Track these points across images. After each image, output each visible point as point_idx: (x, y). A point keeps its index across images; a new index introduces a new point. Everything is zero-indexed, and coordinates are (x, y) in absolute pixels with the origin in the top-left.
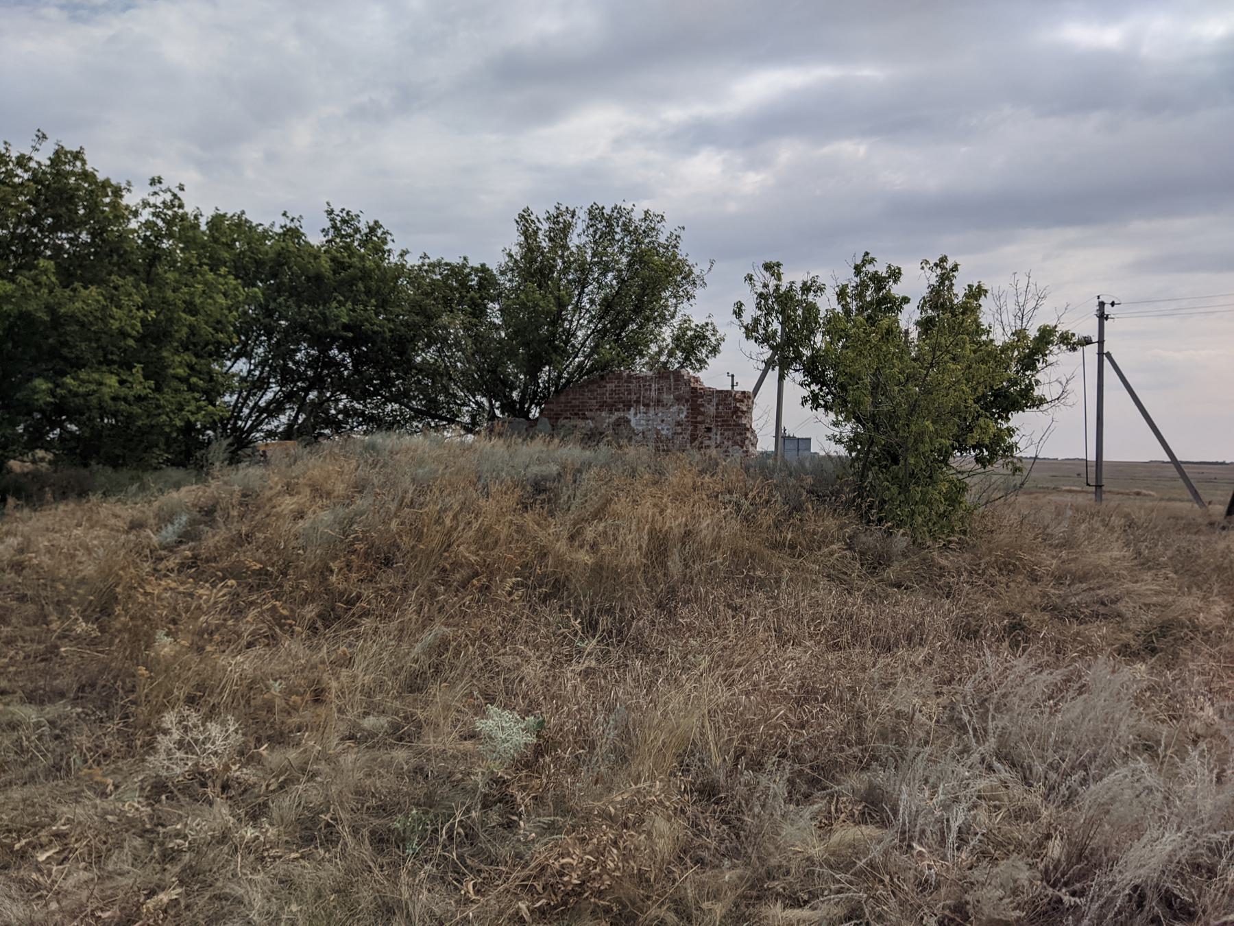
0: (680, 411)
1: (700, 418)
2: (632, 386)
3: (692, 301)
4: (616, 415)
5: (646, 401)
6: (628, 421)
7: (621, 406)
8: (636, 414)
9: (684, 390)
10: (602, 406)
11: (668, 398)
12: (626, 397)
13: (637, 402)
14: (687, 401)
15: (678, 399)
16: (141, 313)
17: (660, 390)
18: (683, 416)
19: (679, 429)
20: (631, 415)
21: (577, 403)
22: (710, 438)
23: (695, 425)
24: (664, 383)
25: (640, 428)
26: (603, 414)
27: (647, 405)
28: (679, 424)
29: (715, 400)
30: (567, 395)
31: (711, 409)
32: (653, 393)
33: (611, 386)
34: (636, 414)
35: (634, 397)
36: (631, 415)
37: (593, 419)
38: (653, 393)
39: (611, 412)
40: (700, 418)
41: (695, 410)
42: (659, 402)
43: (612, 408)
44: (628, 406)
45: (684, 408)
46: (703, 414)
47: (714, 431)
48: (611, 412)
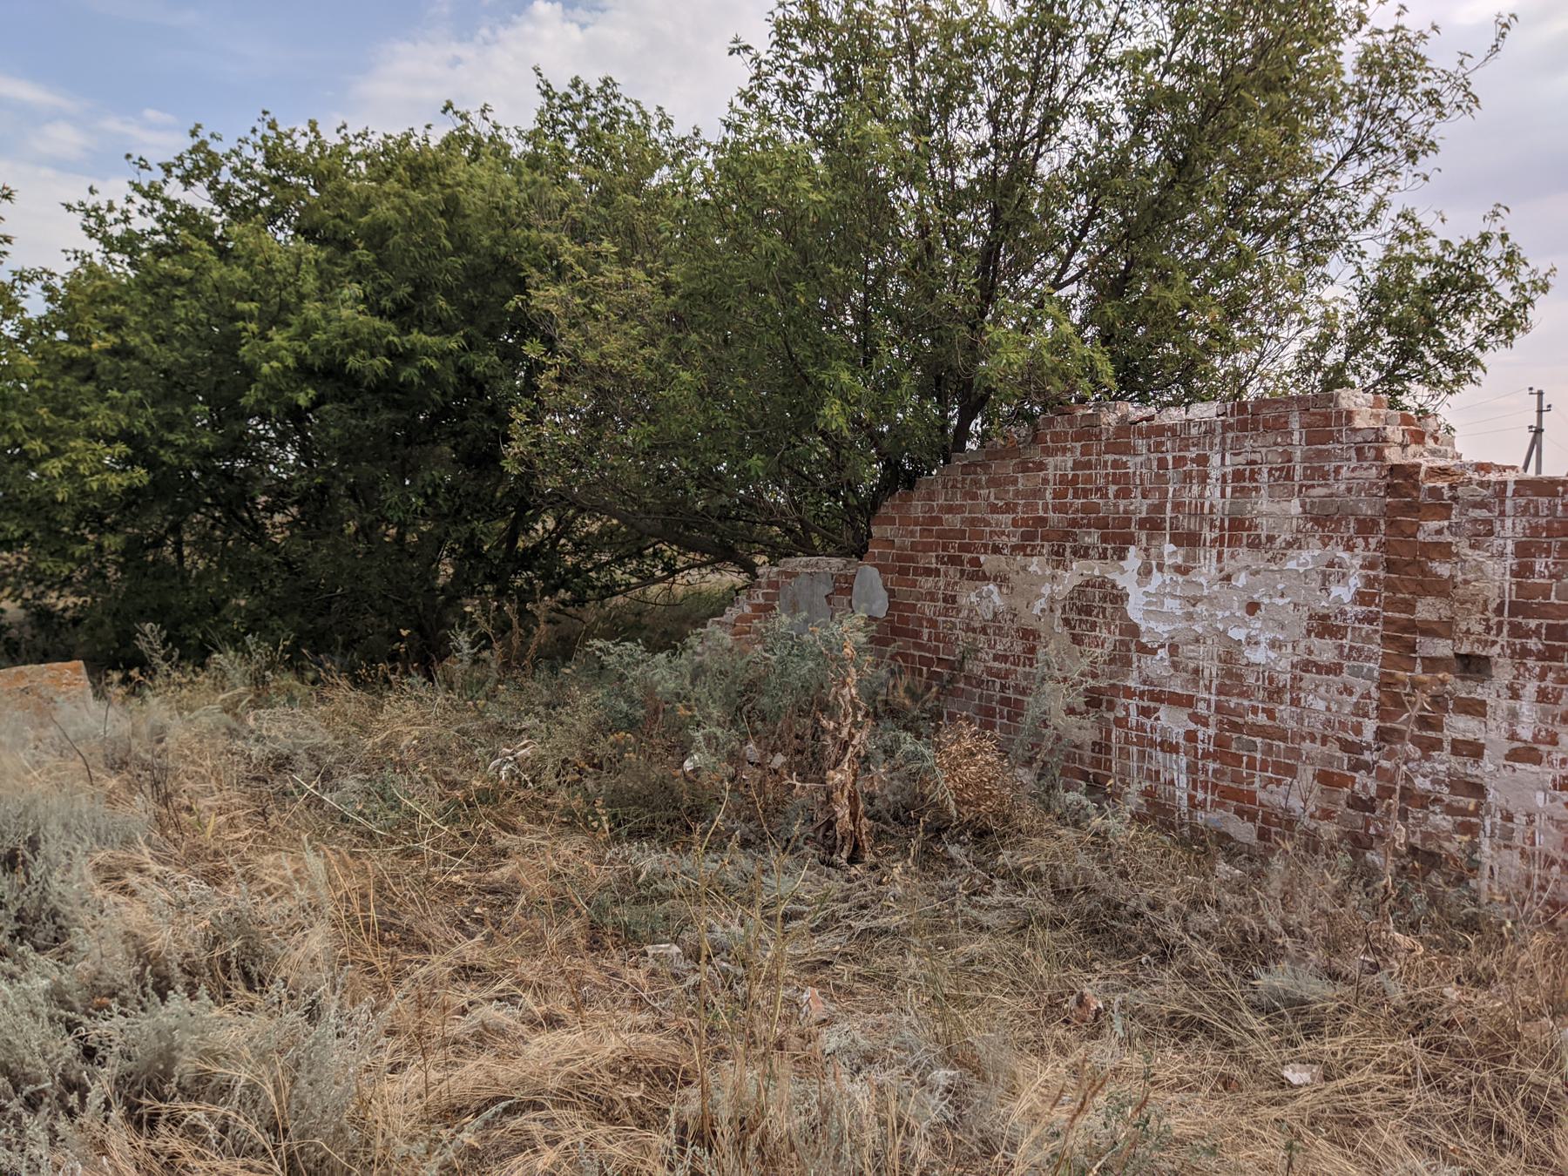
0: (1331, 572)
1: (1427, 609)
2: (1132, 462)
3: (1425, 163)
4: (1076, 572)
5: (1187, 524)
6: (1119, 598)
7: (1092, 538)
8: (1145, 572)
9: (1352, 479)
10: (1032, 535)
11: (1276, 511)
12: (1112, 504)
13: (1153, 525)
14: (1366, 527)
15: (1323, 520)
16: (646, 352)
17: (1242, 480)
18: (1343, 593)
19: (1325, 650)
20: (1126, 573)
21: (953, 521)
22: (1475, 708)
23: (1402, 639)
24: (1260, 449)
25: (1162, 629)
26: (1035, 565)
27: (1188, 540)
28: (1324, 626)
29: (1511, 530)
30: (931, 496)
31: (1491, 572)
32: (1213, 492)
33: (1060, 464)
34: (1145, 572)
35: (1140, 506)
36: (1126, 573)
37: (1001, 579)
38: (1213, 492)
39: (1058, 558)
40: (1427, 609)
41: (1406, 569)
42: (1237, 529)
43: (1064, 545)
44: (1118, 541)
45: (1353, 561)
46: (1443, 588)
47: (1503, 673)
48: (1058, 558)
